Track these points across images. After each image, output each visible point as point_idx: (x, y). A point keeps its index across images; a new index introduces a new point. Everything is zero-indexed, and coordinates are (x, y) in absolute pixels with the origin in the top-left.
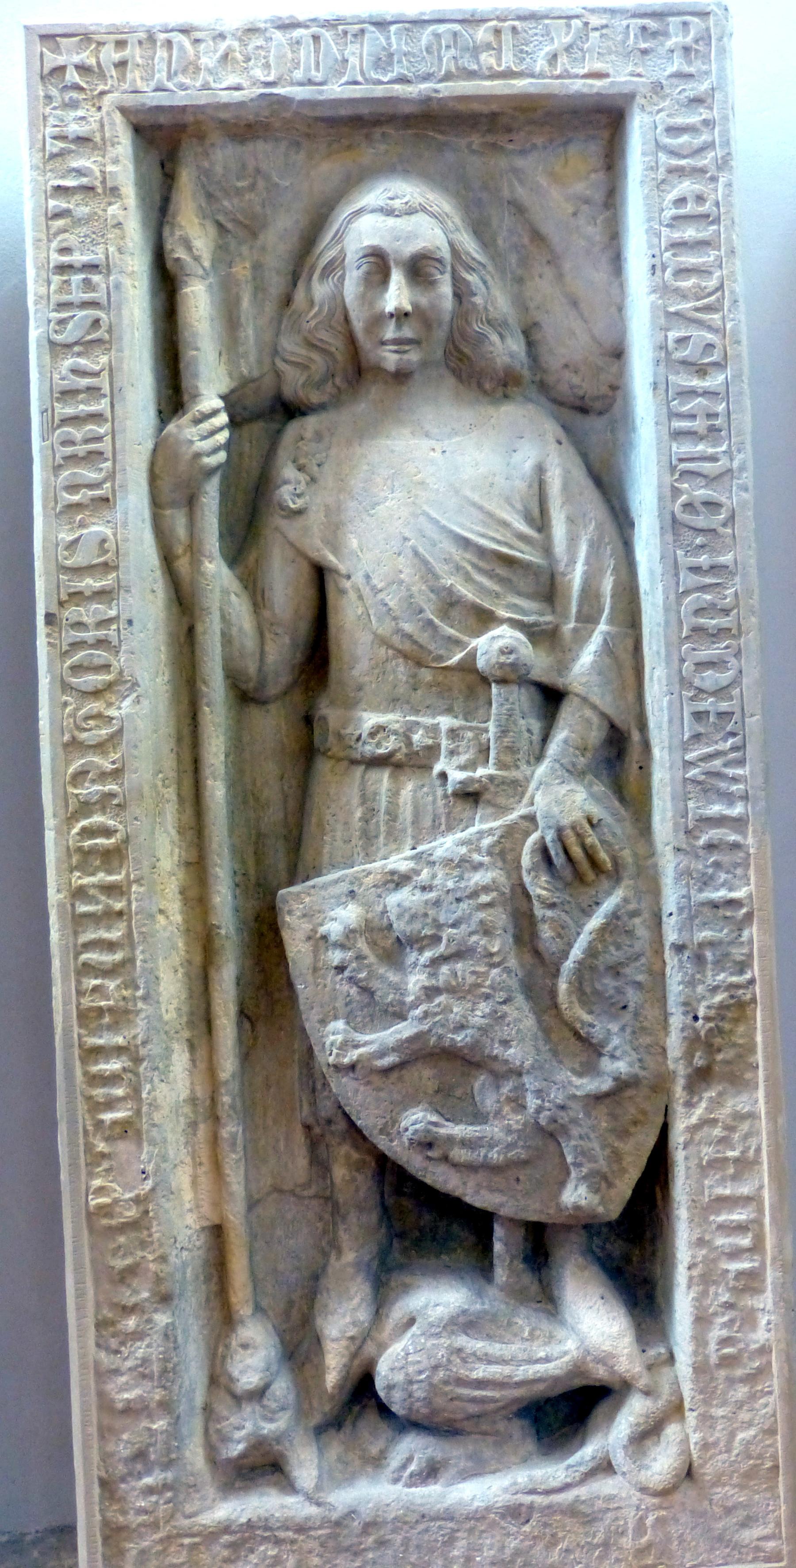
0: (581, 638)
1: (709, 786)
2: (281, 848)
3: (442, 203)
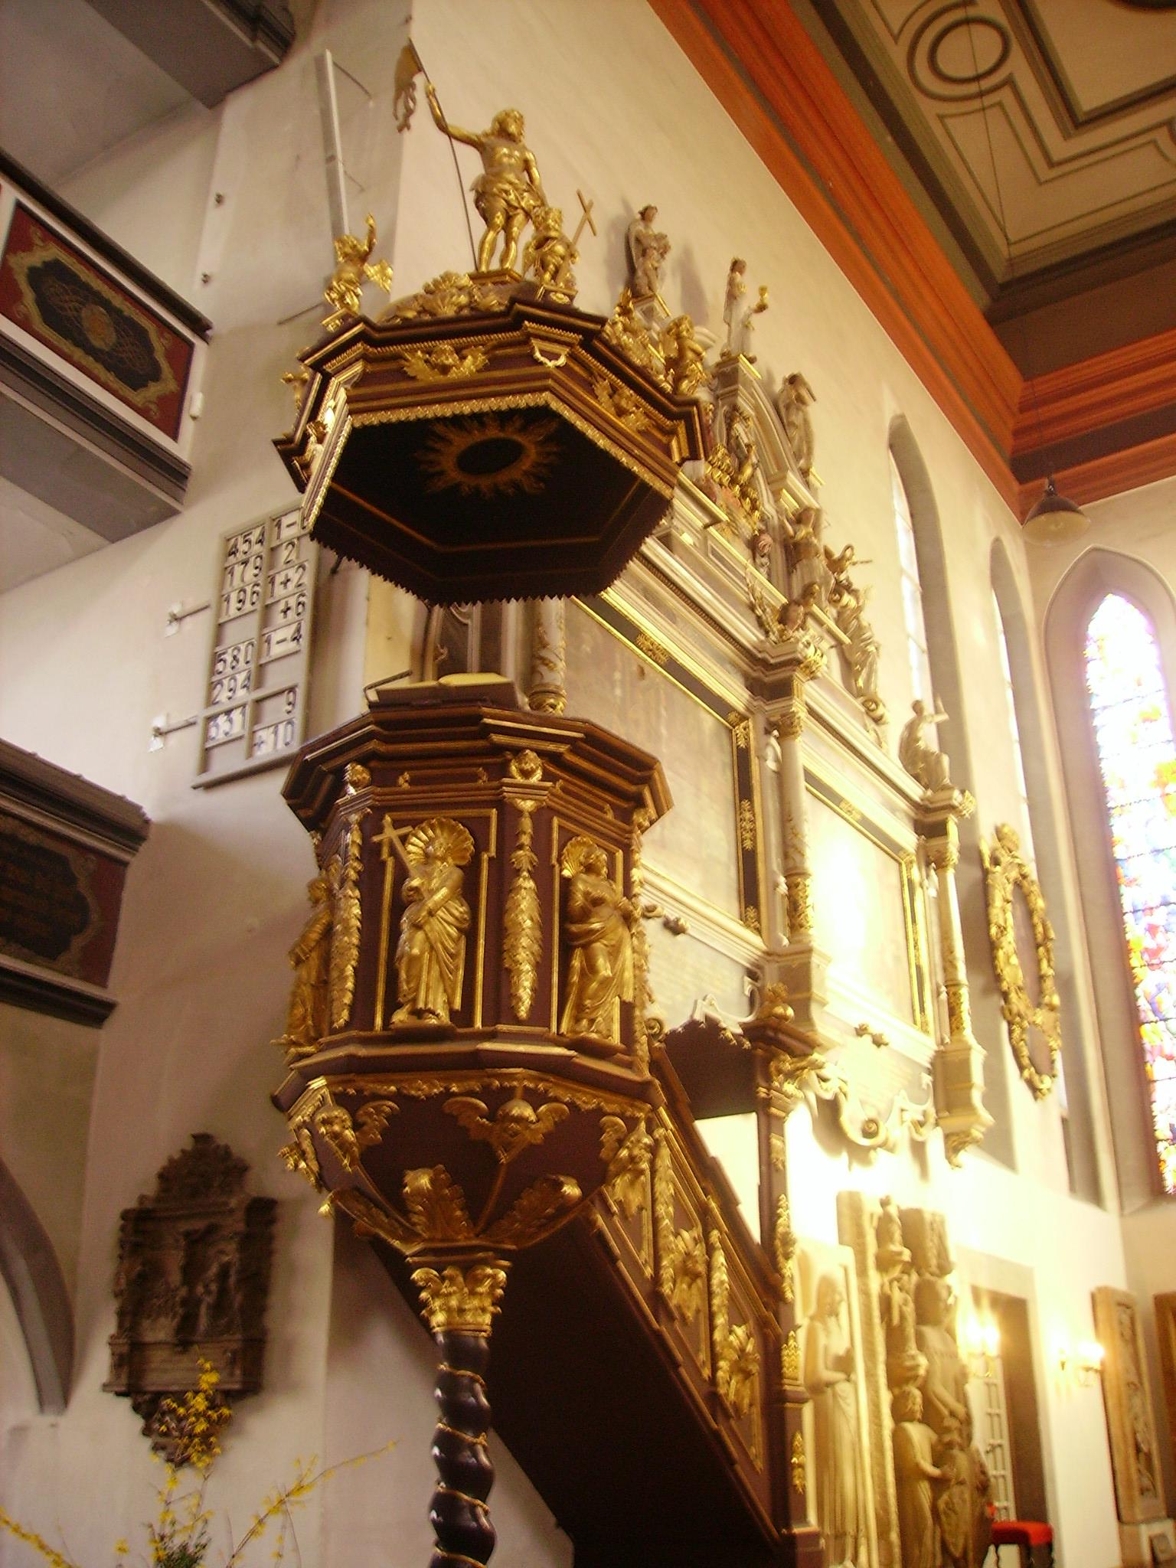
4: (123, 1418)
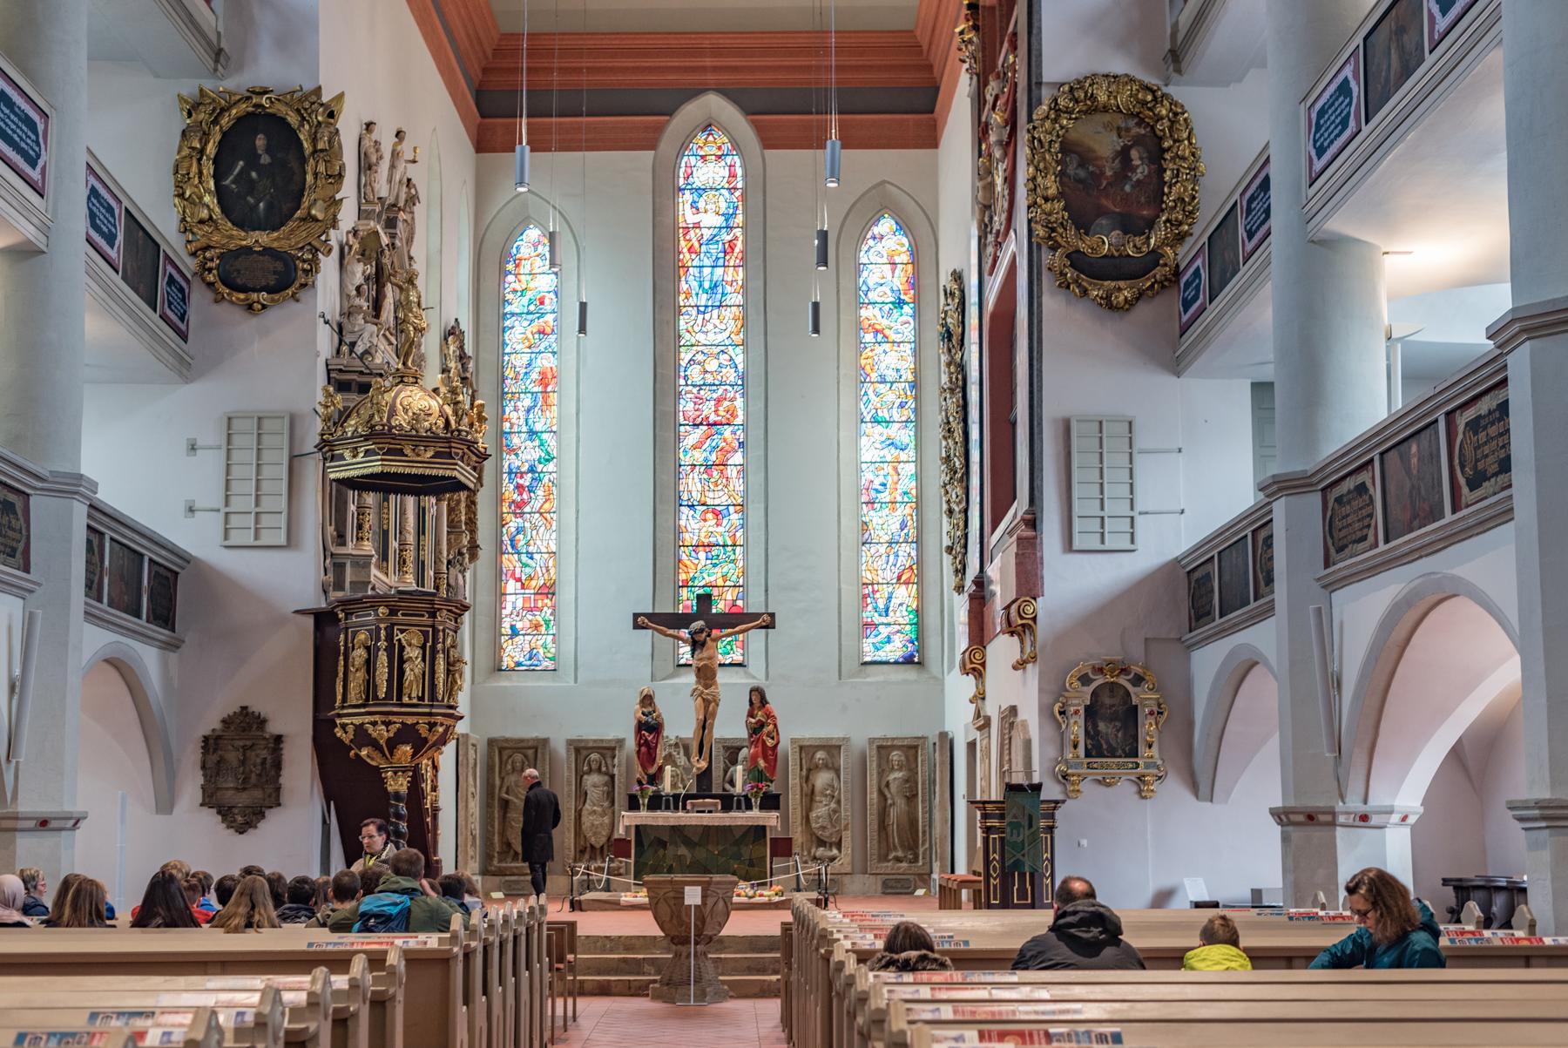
2: (809, 809)
4: (211, 818)
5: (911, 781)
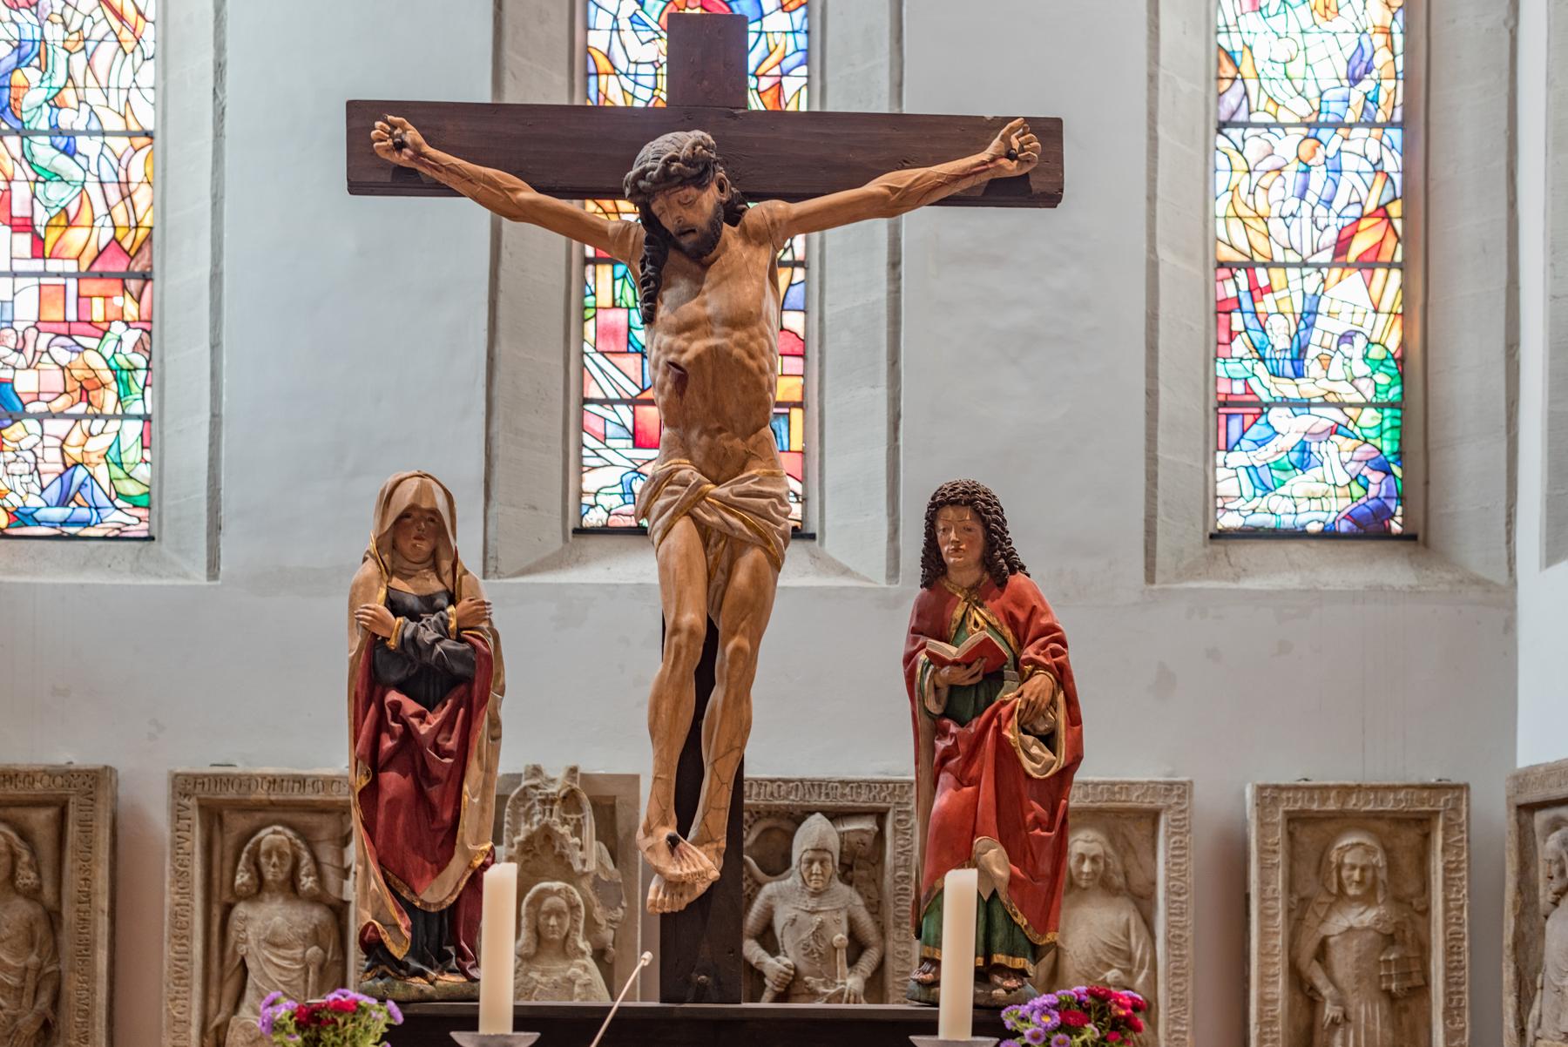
0: (1139, 973)
1: (1176, 1021)
3: (1101, 838)
5: (1404, 941)
